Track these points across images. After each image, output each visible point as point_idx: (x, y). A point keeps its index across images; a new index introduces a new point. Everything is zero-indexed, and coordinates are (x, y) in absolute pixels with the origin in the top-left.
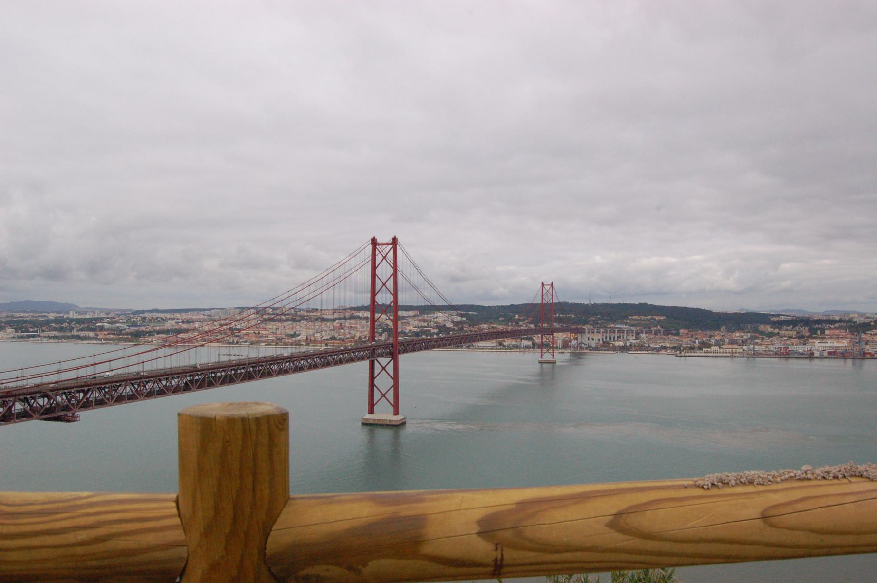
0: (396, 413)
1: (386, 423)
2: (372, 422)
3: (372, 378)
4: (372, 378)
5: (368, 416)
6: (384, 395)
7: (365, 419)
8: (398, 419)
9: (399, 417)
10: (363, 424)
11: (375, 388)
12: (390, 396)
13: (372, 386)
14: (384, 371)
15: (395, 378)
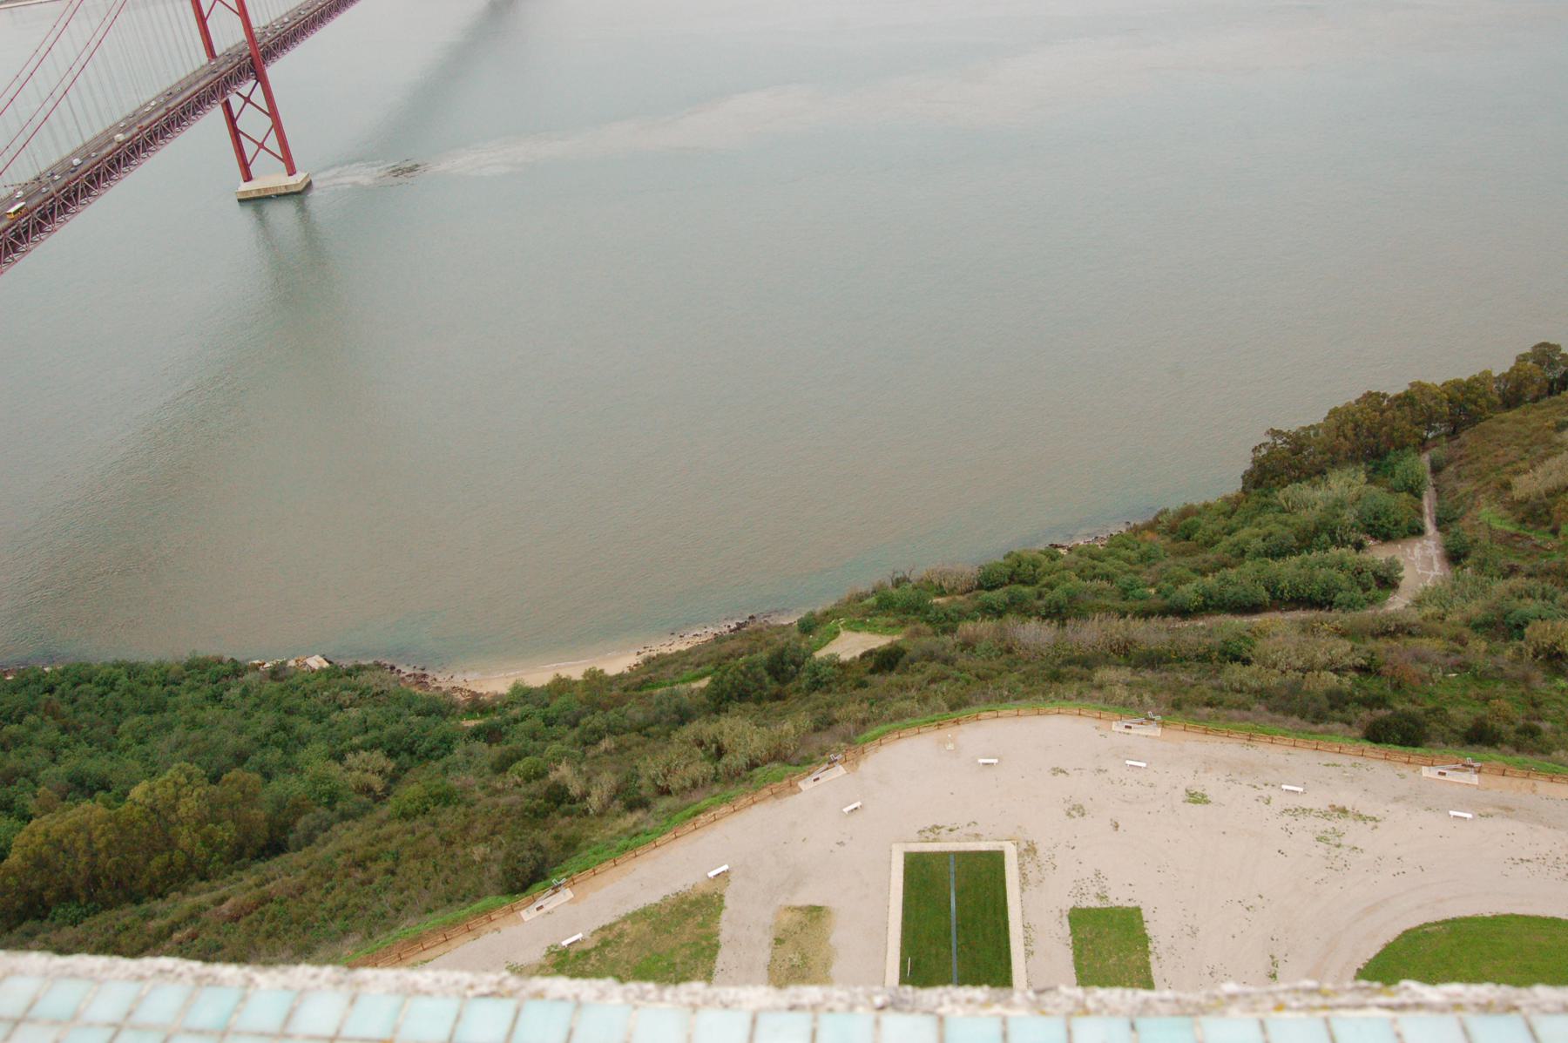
0: (291, 171)
1: (279, 192)
2: (254, 195)
3: (231, 120)
4: (231, 120)
5: (245, 187)
6: (261, 146)
7: (243, 192)
8: (299, 181)
9: (298, 180)
10: (240, 201)
11: (241, 135)
12: (273, 143)
13: (235, 133)
14: (248, 105)
15: (273, 113)
